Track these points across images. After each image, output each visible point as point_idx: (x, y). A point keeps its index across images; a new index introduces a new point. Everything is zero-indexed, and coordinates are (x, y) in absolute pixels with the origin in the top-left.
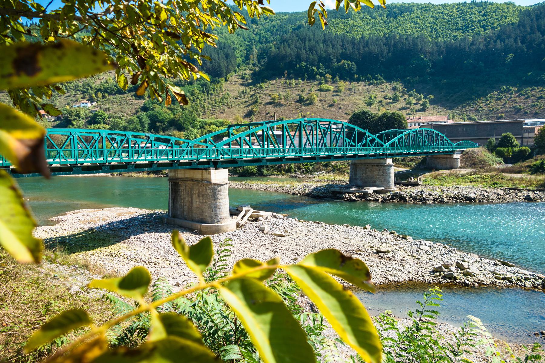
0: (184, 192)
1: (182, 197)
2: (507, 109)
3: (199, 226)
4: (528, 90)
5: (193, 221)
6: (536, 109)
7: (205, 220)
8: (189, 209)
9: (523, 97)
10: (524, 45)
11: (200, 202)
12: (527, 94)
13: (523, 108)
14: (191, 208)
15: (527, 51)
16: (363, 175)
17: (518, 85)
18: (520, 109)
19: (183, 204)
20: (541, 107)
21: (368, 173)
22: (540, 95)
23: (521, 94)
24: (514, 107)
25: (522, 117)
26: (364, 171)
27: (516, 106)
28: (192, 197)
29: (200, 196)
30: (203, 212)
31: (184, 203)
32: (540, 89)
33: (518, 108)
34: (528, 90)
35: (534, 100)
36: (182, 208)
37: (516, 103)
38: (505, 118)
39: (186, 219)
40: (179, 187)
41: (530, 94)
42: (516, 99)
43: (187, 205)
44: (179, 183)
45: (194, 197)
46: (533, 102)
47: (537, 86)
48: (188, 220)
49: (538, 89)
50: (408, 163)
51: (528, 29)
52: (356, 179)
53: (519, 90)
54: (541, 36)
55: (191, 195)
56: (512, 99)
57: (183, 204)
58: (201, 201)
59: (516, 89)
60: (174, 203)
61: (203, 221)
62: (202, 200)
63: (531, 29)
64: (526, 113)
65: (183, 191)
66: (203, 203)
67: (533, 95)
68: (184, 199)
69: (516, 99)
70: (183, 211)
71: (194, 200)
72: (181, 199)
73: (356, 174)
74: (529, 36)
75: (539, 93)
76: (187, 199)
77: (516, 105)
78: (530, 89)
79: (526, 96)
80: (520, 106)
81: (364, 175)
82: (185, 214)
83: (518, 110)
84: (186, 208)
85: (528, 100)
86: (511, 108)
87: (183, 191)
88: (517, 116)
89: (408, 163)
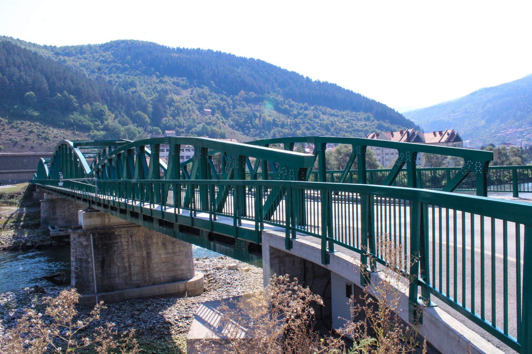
0: (128, 245)
1: (125, 254)
2: (4, 141)
3: (181, 286)
4: (17, 123)
5: (154, 284)
6: (30, 142)
7: (180, 276)
8: (143, 268)
9: (16, 130)
10: (5, 77)
11: (168, 253)
12: (18, 127)
13: (20, 141)
14: (149, 267)
15: (10, 84)
16: (64, 212)
17: (7, 117)
18: (17, 142)
19: (127, 265)
20: (34, 141)
21: (72, 210)
22: (30, 130)
23: (12, 127)
24: (10, 140)
25: (21, 150)
26: (67, 208)
27: (12, 138)
28: (150, 249)
29: (168, 243)
30: (175, 266)
31: (129, 262)
32: (29, 123)
33: (14, 141)
34: (17, 123)
35: (27, 134)
36: (125, 271)
37: (11, 135)
38: (4, 151)
39: (138, 286)
40: (115, 239)
41: (21, 127)
42: (10, 131)
43: (138, 263)
44: (114, 233)
45: (154, 250)
46: (26, 136)
47: (25, 120)
48: (143, 286)
49: (26, 123)
50: (10, 200)
51: (5, 62)
52: (56, 219)
53: (9, 123)
54: (19, 71)
55: (148, 246)
56: (5, 131)
57: (127, 265)
58: (170, 251)
59: (7, 121)
60: (102, 267)
61: (175, 280)
62: (172, 249)
63: (7, 63)
64: (23, 146)
65: (125, 243)
66: (174, 253)
67: (24, 129)
68: (129, 256)
69: (10, 131)
70: (130, 274)
71: (154, 253)
72: (123, 258)
73: (54, 213)
74: (7, 69)
75: (29, 127)
76: (137, 254)
77: (11, 137)
78: (19, 122)
79: (18, 129)
80: (15, 138)
81: (67, 213)
82: (134, 278)
83: (15, 143)
84: (135, 269)
85: (21, 133)
86: (7, 140)
87: (125, 243)
88: (16, 149)
89: (10, 200)
